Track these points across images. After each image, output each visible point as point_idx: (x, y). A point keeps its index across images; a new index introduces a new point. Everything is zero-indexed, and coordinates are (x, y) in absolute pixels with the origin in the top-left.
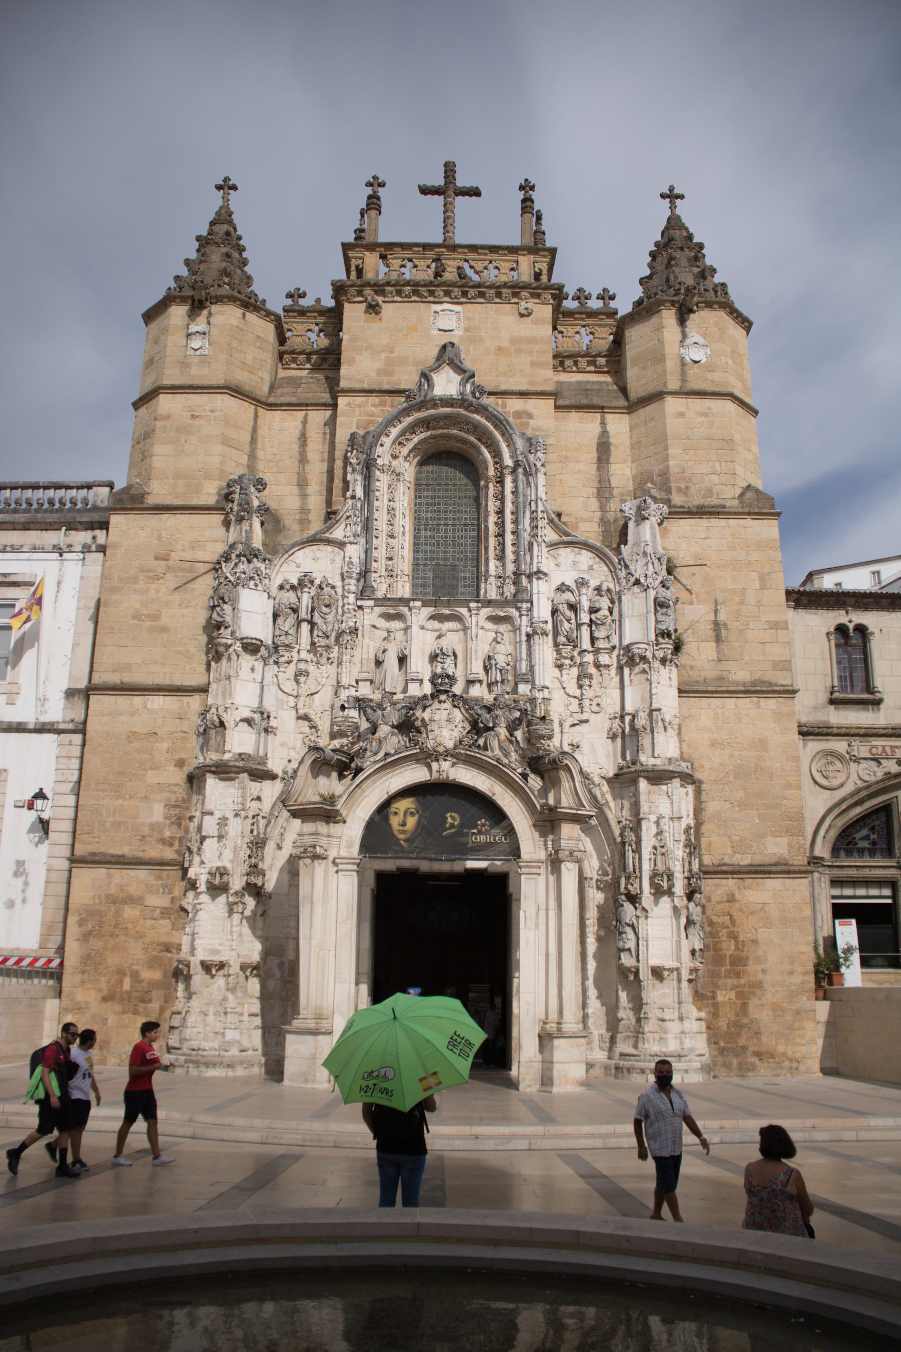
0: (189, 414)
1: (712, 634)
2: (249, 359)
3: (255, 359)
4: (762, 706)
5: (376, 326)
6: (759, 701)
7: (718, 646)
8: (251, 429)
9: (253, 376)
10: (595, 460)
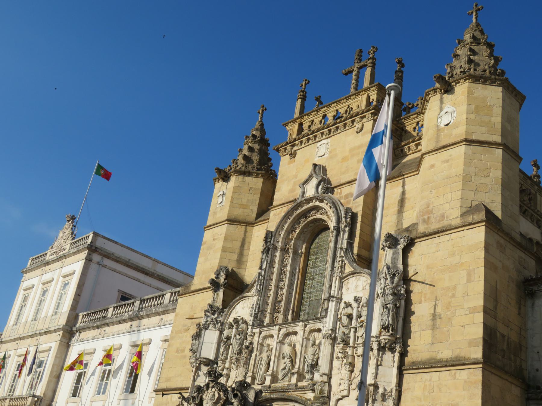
0: (212, 239)
1: (430, 323)
2: (244, 202)
3: (248, 201)
4: (457, 377)
5: (292, 165)
6: (455, 373)
7: (433, 332)
8: (242, 240)
9: (246, 211)
10: (396, 212)
